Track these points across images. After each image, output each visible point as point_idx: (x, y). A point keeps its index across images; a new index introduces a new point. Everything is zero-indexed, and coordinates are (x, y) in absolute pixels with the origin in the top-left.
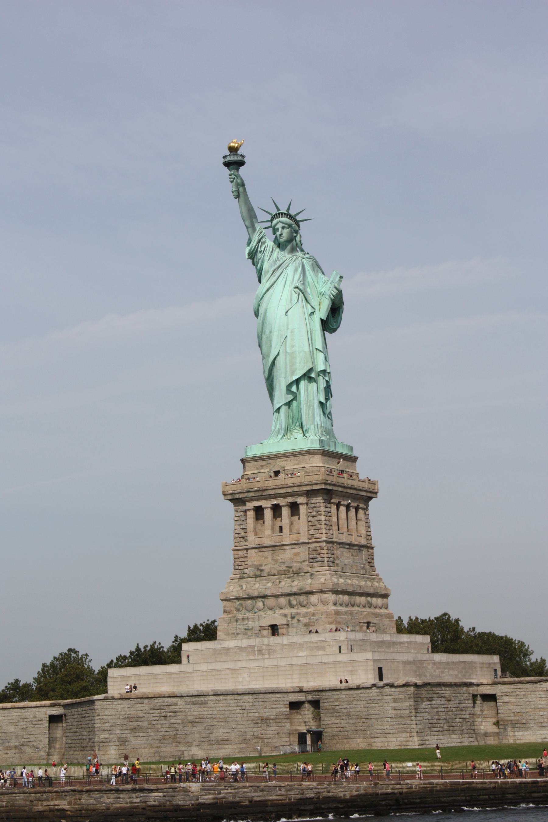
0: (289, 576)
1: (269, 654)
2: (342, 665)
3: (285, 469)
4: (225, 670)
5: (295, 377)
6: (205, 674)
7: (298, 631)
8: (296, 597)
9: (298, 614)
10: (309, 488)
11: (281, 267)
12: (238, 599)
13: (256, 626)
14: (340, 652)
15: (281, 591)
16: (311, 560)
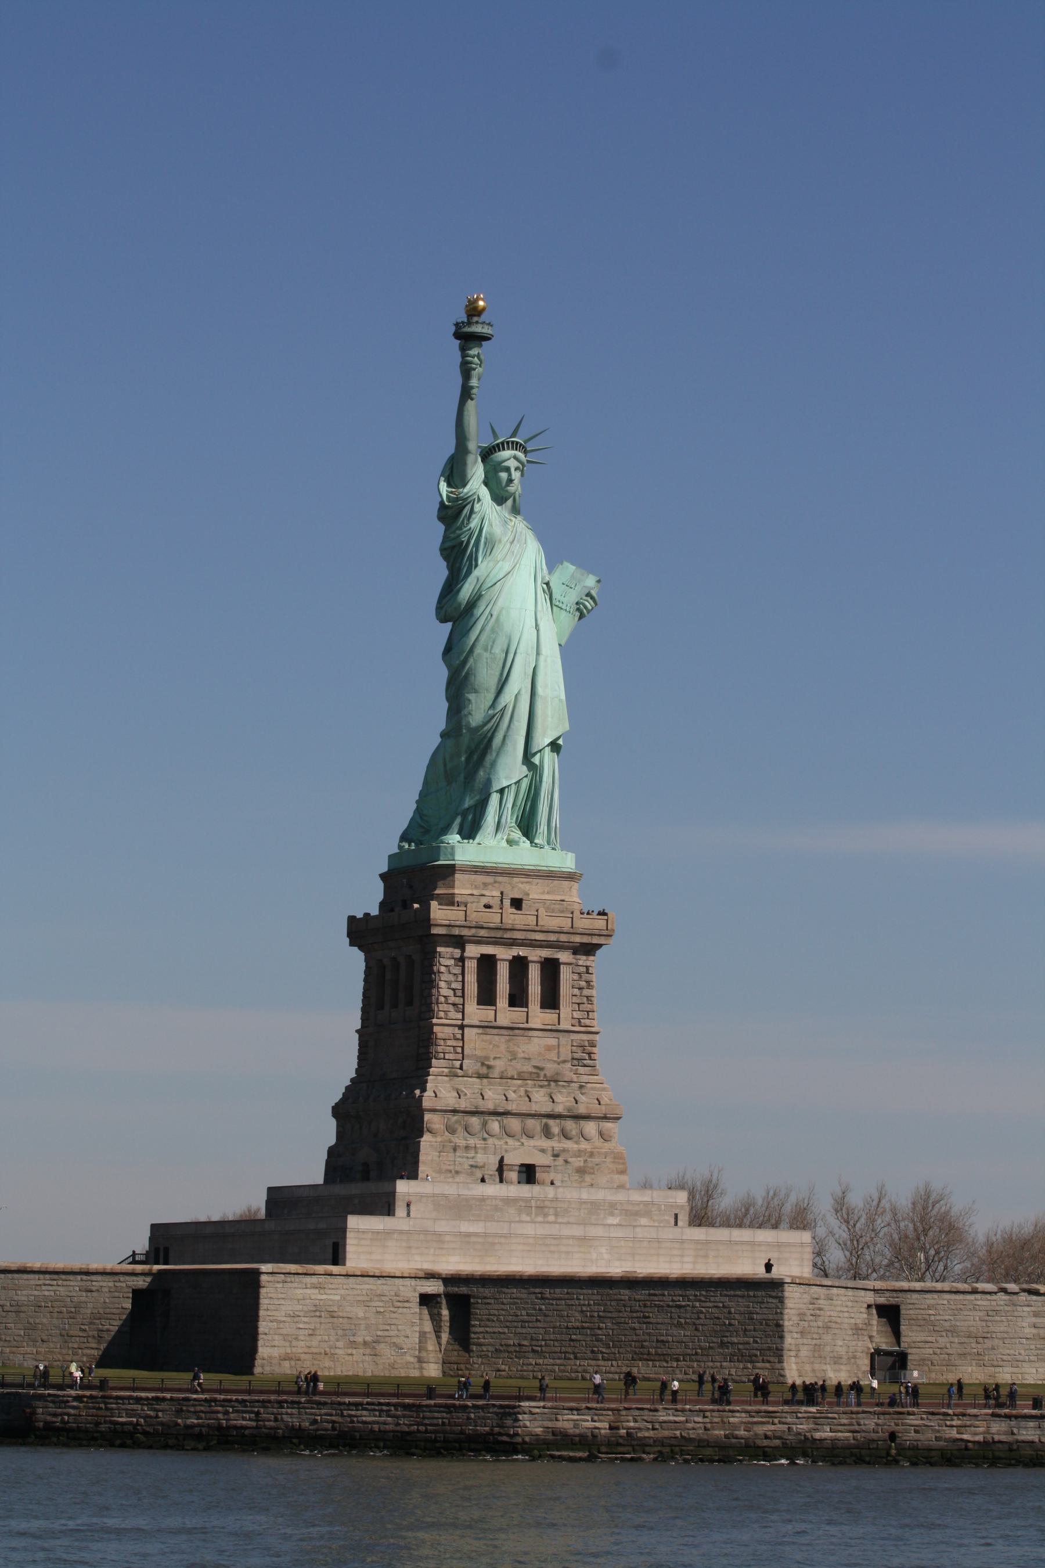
0: (541, 1083)
1: (556, 1215)
2: (763, 1248)
3: (531, 897)
4: (568, 1238)
5: (548, 741)
6: (531, 1241)
7: (566, 1179)
8: (558, 1121)
9: (564, 1150)
10: (586, 940)
11: (516, 539)
12: (455, 1111)
13: (490, 1162)
14: (676, 1224)
15: (535, 1108)
16: (576, 1062)
